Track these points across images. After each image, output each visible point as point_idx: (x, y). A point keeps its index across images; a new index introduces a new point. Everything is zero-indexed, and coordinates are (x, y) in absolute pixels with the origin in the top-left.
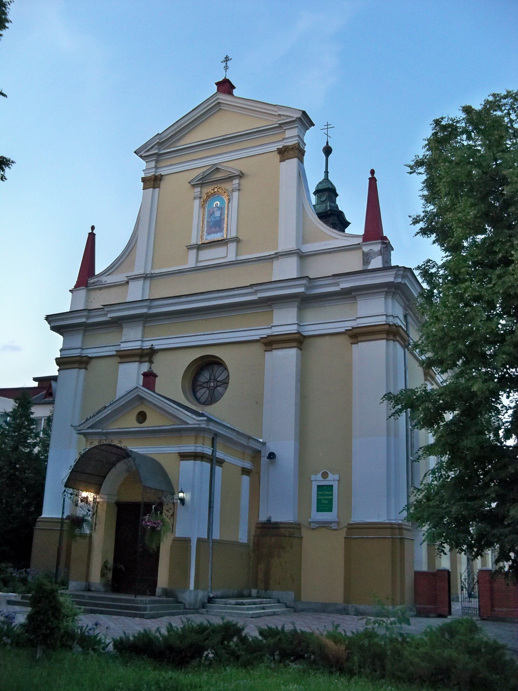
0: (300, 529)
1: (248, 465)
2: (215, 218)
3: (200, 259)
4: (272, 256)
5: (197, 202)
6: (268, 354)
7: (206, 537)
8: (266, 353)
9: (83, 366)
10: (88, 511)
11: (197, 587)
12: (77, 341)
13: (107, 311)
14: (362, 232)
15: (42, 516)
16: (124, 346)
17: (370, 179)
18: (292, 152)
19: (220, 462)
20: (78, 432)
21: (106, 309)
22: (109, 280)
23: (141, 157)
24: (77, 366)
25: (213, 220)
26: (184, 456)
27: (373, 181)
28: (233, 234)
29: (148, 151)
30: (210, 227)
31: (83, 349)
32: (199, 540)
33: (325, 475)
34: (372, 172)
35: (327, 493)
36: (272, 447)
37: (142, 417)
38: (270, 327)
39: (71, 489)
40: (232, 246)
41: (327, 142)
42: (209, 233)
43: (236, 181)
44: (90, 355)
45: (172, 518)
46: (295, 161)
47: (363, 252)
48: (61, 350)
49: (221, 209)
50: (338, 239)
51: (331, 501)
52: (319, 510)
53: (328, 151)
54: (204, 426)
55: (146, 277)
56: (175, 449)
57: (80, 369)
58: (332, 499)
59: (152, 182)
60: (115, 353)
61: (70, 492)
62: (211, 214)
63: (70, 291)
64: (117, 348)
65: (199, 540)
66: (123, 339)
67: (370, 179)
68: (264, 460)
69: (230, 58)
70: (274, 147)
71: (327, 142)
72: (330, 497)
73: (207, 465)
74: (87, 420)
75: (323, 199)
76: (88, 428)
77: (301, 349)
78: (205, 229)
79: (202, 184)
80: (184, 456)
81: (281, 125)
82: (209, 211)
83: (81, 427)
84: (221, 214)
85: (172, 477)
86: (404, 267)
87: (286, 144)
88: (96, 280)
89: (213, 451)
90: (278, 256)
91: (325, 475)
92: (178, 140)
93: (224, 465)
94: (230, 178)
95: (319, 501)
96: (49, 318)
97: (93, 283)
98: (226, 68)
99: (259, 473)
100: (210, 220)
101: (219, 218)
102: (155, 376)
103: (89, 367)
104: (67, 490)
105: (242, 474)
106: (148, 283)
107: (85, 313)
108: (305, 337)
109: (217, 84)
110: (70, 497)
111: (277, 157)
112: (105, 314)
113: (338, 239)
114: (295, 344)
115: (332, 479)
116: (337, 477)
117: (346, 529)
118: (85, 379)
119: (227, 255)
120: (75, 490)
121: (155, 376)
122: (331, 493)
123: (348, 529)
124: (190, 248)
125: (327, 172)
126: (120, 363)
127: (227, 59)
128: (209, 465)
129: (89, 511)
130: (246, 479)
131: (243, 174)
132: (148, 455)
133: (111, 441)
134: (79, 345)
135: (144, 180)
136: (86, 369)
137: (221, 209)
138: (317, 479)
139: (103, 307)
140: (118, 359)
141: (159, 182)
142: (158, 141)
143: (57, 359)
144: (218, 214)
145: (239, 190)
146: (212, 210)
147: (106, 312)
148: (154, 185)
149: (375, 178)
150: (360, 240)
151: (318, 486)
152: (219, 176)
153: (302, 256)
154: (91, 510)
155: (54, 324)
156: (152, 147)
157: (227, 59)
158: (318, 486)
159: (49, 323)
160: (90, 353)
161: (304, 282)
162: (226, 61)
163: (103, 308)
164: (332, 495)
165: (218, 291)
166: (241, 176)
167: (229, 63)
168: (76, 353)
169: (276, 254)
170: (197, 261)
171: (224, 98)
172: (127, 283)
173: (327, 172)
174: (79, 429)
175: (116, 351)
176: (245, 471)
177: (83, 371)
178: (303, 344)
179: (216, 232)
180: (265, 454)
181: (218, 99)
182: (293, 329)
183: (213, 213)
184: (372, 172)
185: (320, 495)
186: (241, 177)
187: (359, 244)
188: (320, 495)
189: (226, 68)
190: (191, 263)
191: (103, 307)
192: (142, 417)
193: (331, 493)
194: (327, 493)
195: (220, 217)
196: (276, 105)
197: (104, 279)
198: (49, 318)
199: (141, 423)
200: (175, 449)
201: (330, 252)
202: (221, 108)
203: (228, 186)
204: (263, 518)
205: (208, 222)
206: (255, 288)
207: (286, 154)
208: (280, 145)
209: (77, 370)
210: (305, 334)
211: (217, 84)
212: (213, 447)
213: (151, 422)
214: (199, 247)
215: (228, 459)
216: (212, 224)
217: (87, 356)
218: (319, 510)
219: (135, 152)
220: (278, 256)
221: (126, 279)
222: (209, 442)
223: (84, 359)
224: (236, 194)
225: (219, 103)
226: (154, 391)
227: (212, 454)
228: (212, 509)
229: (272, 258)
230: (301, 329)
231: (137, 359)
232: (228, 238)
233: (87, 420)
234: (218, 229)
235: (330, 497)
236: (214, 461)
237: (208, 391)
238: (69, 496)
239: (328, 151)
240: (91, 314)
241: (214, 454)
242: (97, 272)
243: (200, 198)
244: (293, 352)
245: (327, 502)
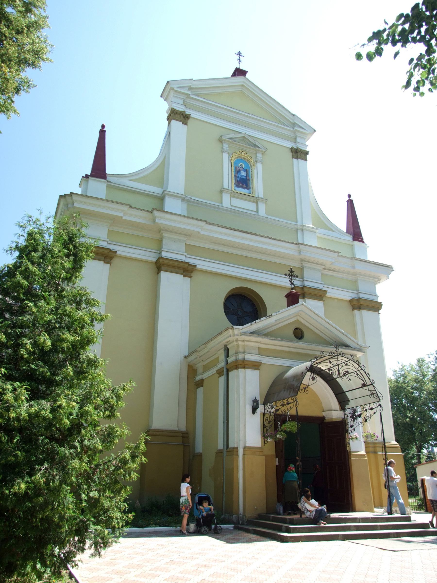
2: (242, 176)
25: (240, 176)
50: (336, 232)
79: (230, 142)
84: (246, 175)
101: (245, 178)
113: (336, 232)
136: (110, 264)
142: (191, 85)
179: (244, 188)
181: (244, 82)
183: (239, 171)
189: (239, 61)
196: (294, 115)
205: (235, 176)
216: (239, 179)
234: (245, 186)
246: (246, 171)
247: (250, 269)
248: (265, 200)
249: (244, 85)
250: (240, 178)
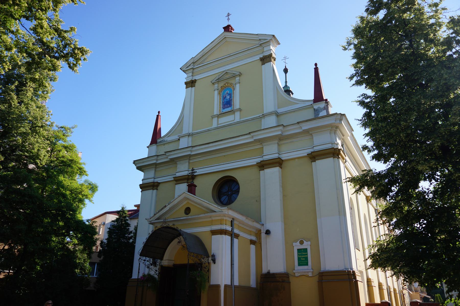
0: (288, 277)
1: (254, 238)
2: (227, 99)
3: (219, 123)
4: (261, 117)
5: (216, 92)
6: (261, 172)
7: (230, 284)
8: (261, 171)
9: (155, 188)
10: (155, 271)
12: (151, 173)
13: (169, 155)
14: (312, 98)
15: (132, 278)
16: (178, 175)
17: (315, 68)
19: (237, 236)
20: (149, 223)
21: (167, 154)
22: (169, 139)
23: (184, 71)
24: (151, 188)
25: (226, 101)
26: (214, 232)
27: (316, 70)
29: (188, 67)
30: (224, 105)
31: (155, 178)
32: (226, 286)
33: (302, 243)
34: (316, 65)
35: (304, 253)
36: (268, 226)
38: (262, 156)
39: (144, 257)
40: (237, 114)
41: (286, 66)
42: (224, 108)
43: (237, 78)
44: (159, 182)
45: (208, 272)
47: (314, 109)
48: (143, 180)
49: (230, 95)
51: (307, 258)
52: (299, 265)
53: (286, 71)
55: (189, 135)
56: (208, 229)
57: (153, 189)
58: (307, 257)
59: (191, 84)
60: (173, 179)
61: (143, 259)
62: (224, 98)
63: (147, 147)
64: (174, 176)
65: (226, 286)
66: (178, 171)
67: (315, 68)
68: (263, 235)
69: (230, 14)
70: (258, 58)
71: (286, 66)
72: (306, 256)
74: (155, 215)
76: (155, 220)
77: (281, 168)
78: (222, 106)
79: (218, 82)
80: (214, 232)
81: (261, 44)
82: (223, 96)
83: (152, 219)
85: (207, 246)
86: (341, 114)
87: (265, 55)
88: (161, 140)
89: (232, 229)
90: (264, 116)
91: (302, 243)
92: (204, 60)
93: (239, 238)
94: (234, 76)
95: (299, 259)
96: (135, 162)
97: (160, 142)
98: (228, 19)
99: (261, 244)
100: (224, 101)
102: (196, 186)
103: (159, 188)
104: (141, 258)
105: (250, 244)
106: (190, 138)
107: (155, 158)
108: (283, 161)
109: (224, 28)
110: (144, 263)
111: (260, 63)
112: (166, 157)
114: (278, 165)
115: (307, 245)
116: (309, 243)
117: (318, 276)
118: (156, 195)
119: (235, 120)
120: (147, 258)
121: (196, 186)
122: (306, 253)
123: (320, 276)
124: (213, 117)
125: (286, 82)
126: (176, 184)
127: (229, 15)
128: (230, 237)
129: (156, 271)
130: (253, 247)
131: (241, 74)
132: (193, 234)
133: (168, 225)
134: (153, 176)
135: (186, 83)
136: (157, 189)
138: (297, 246)
139: (165, 153)
140: (175, 182)
141: (194, 84)
143: (140, 185)
144: (228, 97)
145: (239, 83)
146: (225, 96)
147: (167, 156)
148: (192, 85)
149: (318, 67)
150: (312, 102)
151: (298, 249)
152: (227, 76)
153: (278, 115)
154: (158, 270)
155: (138, 165)
156: (190, 65)
157: (229, 15)
158: (298, 249)
159: (136, 165)
160: (159, 180)
161: (281, 128)
162: (228, 16)
163: (165, 154)
164: (307, 254)
165: (231, 138)
166: (240, 75)
167: (230, 17)
168: (151, 180)
169: (263, 115)
170: (218, 124)
171: (227, 34)
172: (179, 140)
173: (286, 82)
174: (150, 220)
175: (173, 177)
176: (252, 242)
177: (155, 191)
178: (282, 165)
179: (228, 107)
180: (263, 231)
181: (225, 35)
182: (276, 156)
183: (226, 97)
184: (316, 65)
185: (300, 255)
186: (240, 76)
187: (311, 104)
188: (300, 255)
189: (228, 19)
190: (215, 125)
191: (165, 153)
193: (306, 253)
194: (304, 253)
195: (229, 99)
196: (258, 34)
197: (166, 139)
198: (135, 162)
199: (187, 214)
201: (294, 111)
202: (227, 40)
203: (232, 81)
204: (265, 271)
205: (223, 102)
206: (252, 134)
207: (265, 60)
209: (152, 190)
210: (283, 159)
211: (224, 28)
212: (232, 226)
214: (218, 116)
215: (241, 234)
217: (157, 182)
218: (299, 265)
219: (180, 69)
220: (264, 116)
221: (178, 138)
223: (156, 184)
224: (238, 86)
225: (225, 37)
226: (195, 195)
227: (232, 230)
228: (233, 265)
229: (261, 118)
230: (280, 156)
232: (235, 109)
233: (155, 215)
234: (229, 106)
235: (306, 256)
236: (233, 236)
237: (227, 197)
238: (143, 261)
239: (286, 71)
240: (159, 158)
241: (232, 230)
242: (162, 135)
243: (218, 89)
244: (276, 170)
245: (304, 259)
247: (232, 162)
249: (226, 36)
250: (226, 101)
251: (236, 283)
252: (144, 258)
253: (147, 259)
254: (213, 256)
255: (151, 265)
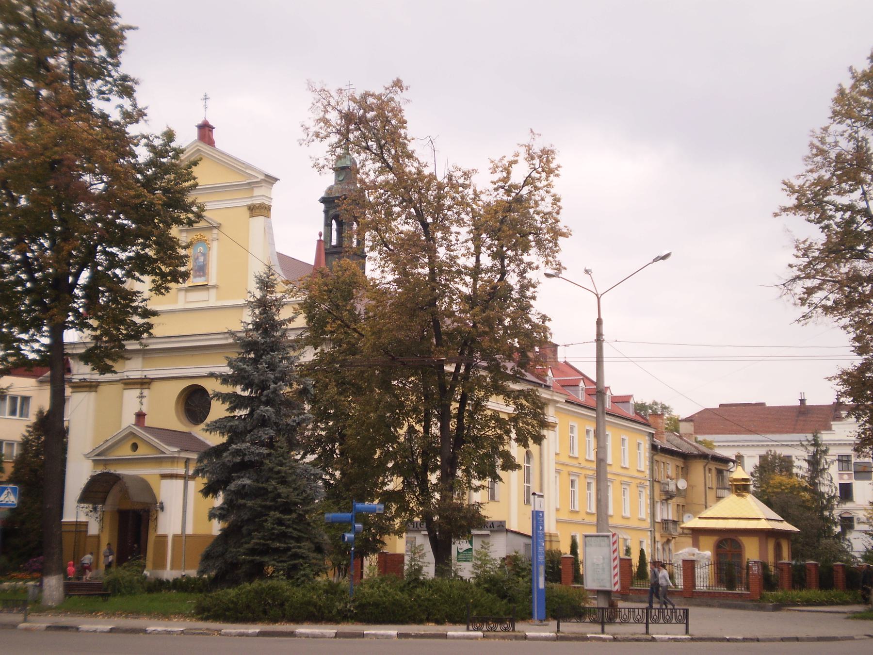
9: (94, 389)
11: (172, 568)
18: (258, 211)
28: (212, 282)
37: (135, 447)
40: (213, 292)
43: (215, 231)
46: (261, 219)
54: (177, 455)
73: (180, 483)
75: (341, 178)
80: (164, 476)
81: (249, 184)
85: (155, 491)
87: (255, 202)
111: (247, 213)
127: (206, 98)
131: (220, 224)
132: (141, 476)
136: (96, 391)
137: (204, 255)
140: (121, 386)
144: (201, 259)
157: (206, 98)
167: (207, 101)
177: (93, 394)
179: (200, 276)
181: (197, 146)
183: (197, 258)
192: (135, 447)
200: (157, 471)
208: (249, 202)
213: (142, 452)
222: (183, 465)
225: (198, 149)
231: (139, 386)
246: (204, 255)
248: (215, 287)
251: (189, 531)
252: (82, 505)
253: (86, 505)
254: (162, 503)
255: (91, 511)
